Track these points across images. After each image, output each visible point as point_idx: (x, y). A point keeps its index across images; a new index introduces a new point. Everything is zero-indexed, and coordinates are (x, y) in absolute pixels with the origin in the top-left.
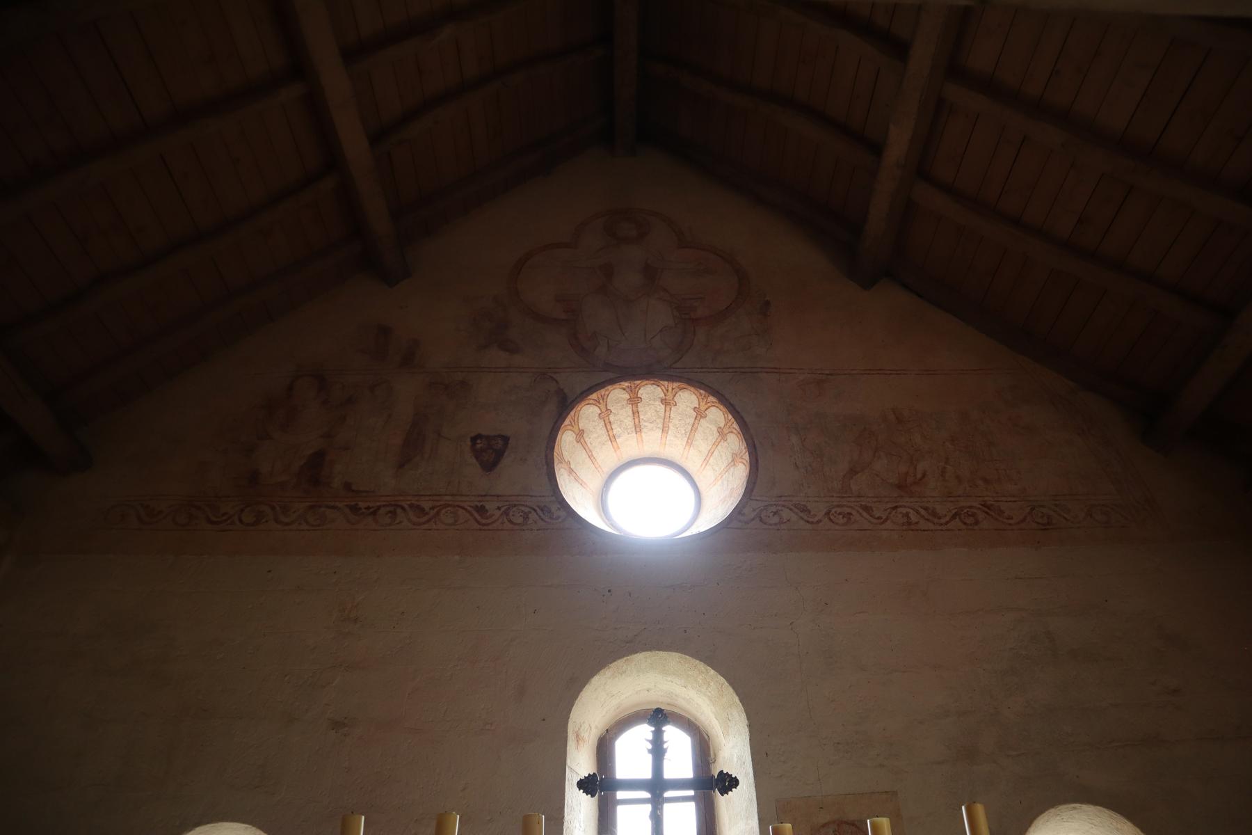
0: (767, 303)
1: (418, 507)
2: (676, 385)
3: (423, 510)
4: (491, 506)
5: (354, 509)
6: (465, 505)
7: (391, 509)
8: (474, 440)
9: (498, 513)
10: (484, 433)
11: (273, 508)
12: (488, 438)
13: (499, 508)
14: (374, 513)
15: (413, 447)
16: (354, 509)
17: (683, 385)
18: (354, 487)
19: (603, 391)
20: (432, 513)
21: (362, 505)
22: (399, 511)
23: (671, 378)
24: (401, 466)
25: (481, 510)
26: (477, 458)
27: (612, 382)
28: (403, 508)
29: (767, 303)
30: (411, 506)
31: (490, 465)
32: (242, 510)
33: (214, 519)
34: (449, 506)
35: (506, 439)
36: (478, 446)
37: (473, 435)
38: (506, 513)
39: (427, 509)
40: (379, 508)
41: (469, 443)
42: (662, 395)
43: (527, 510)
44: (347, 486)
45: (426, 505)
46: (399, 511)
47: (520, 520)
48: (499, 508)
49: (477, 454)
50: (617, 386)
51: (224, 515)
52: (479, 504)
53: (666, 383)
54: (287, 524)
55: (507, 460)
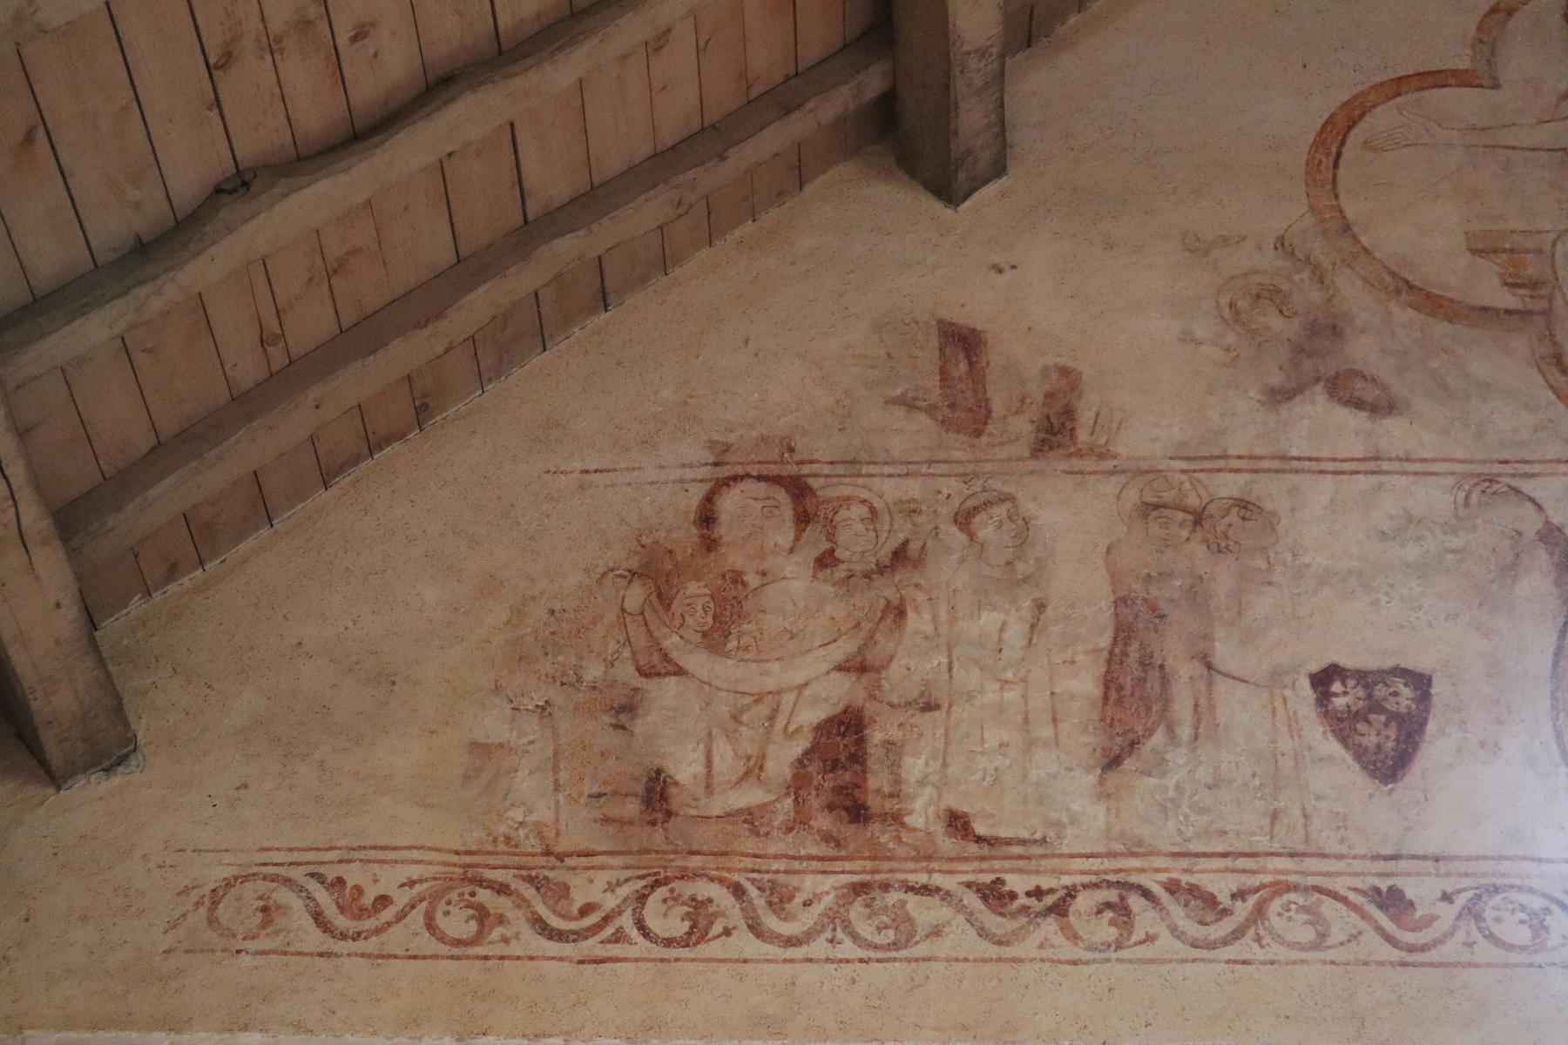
1: (1193, 890)
3: (1211, 901)
4: (1421, 889)
5: (995, 895)
6: (1339, 885)
7: (1112, 895)
8: (1323, 680)
9: (1448, 912)
10: (1347, 662)
11: (738, 891)
12: (1363, 677)
13: (1447, 897)
14: (1059, 909)
15: (1132, 707)
16: (995, 895)
18: (980, 829)
20: (1243, 909)
21: (1014, 882)
22: (1135, 902)
24: (1112, 762)
25: (1392, 900)
26: (1344, 741)
28: (1146, 894)
30: (1172, 888)
31: (1390, 766)
32: (642, 898)
33: (555, 922)
34: (1295, 888)
35: (1421, 683)
36: (1339, 702)
37: (1315, 667)
38: (1472, 912)
39: (1224, 899)
40: (1071, 892)
41: (1307, 692)
43: (1536, 903)
44: (958, 823)
45: (1221, 886)
46: (1135, 902)
47: (1523, 935)
48: (1447, 897)
49: (1343, 726)
51: (586, 910)
52: (1384, 885)
54: (791, 942)
55: (1436, 747)
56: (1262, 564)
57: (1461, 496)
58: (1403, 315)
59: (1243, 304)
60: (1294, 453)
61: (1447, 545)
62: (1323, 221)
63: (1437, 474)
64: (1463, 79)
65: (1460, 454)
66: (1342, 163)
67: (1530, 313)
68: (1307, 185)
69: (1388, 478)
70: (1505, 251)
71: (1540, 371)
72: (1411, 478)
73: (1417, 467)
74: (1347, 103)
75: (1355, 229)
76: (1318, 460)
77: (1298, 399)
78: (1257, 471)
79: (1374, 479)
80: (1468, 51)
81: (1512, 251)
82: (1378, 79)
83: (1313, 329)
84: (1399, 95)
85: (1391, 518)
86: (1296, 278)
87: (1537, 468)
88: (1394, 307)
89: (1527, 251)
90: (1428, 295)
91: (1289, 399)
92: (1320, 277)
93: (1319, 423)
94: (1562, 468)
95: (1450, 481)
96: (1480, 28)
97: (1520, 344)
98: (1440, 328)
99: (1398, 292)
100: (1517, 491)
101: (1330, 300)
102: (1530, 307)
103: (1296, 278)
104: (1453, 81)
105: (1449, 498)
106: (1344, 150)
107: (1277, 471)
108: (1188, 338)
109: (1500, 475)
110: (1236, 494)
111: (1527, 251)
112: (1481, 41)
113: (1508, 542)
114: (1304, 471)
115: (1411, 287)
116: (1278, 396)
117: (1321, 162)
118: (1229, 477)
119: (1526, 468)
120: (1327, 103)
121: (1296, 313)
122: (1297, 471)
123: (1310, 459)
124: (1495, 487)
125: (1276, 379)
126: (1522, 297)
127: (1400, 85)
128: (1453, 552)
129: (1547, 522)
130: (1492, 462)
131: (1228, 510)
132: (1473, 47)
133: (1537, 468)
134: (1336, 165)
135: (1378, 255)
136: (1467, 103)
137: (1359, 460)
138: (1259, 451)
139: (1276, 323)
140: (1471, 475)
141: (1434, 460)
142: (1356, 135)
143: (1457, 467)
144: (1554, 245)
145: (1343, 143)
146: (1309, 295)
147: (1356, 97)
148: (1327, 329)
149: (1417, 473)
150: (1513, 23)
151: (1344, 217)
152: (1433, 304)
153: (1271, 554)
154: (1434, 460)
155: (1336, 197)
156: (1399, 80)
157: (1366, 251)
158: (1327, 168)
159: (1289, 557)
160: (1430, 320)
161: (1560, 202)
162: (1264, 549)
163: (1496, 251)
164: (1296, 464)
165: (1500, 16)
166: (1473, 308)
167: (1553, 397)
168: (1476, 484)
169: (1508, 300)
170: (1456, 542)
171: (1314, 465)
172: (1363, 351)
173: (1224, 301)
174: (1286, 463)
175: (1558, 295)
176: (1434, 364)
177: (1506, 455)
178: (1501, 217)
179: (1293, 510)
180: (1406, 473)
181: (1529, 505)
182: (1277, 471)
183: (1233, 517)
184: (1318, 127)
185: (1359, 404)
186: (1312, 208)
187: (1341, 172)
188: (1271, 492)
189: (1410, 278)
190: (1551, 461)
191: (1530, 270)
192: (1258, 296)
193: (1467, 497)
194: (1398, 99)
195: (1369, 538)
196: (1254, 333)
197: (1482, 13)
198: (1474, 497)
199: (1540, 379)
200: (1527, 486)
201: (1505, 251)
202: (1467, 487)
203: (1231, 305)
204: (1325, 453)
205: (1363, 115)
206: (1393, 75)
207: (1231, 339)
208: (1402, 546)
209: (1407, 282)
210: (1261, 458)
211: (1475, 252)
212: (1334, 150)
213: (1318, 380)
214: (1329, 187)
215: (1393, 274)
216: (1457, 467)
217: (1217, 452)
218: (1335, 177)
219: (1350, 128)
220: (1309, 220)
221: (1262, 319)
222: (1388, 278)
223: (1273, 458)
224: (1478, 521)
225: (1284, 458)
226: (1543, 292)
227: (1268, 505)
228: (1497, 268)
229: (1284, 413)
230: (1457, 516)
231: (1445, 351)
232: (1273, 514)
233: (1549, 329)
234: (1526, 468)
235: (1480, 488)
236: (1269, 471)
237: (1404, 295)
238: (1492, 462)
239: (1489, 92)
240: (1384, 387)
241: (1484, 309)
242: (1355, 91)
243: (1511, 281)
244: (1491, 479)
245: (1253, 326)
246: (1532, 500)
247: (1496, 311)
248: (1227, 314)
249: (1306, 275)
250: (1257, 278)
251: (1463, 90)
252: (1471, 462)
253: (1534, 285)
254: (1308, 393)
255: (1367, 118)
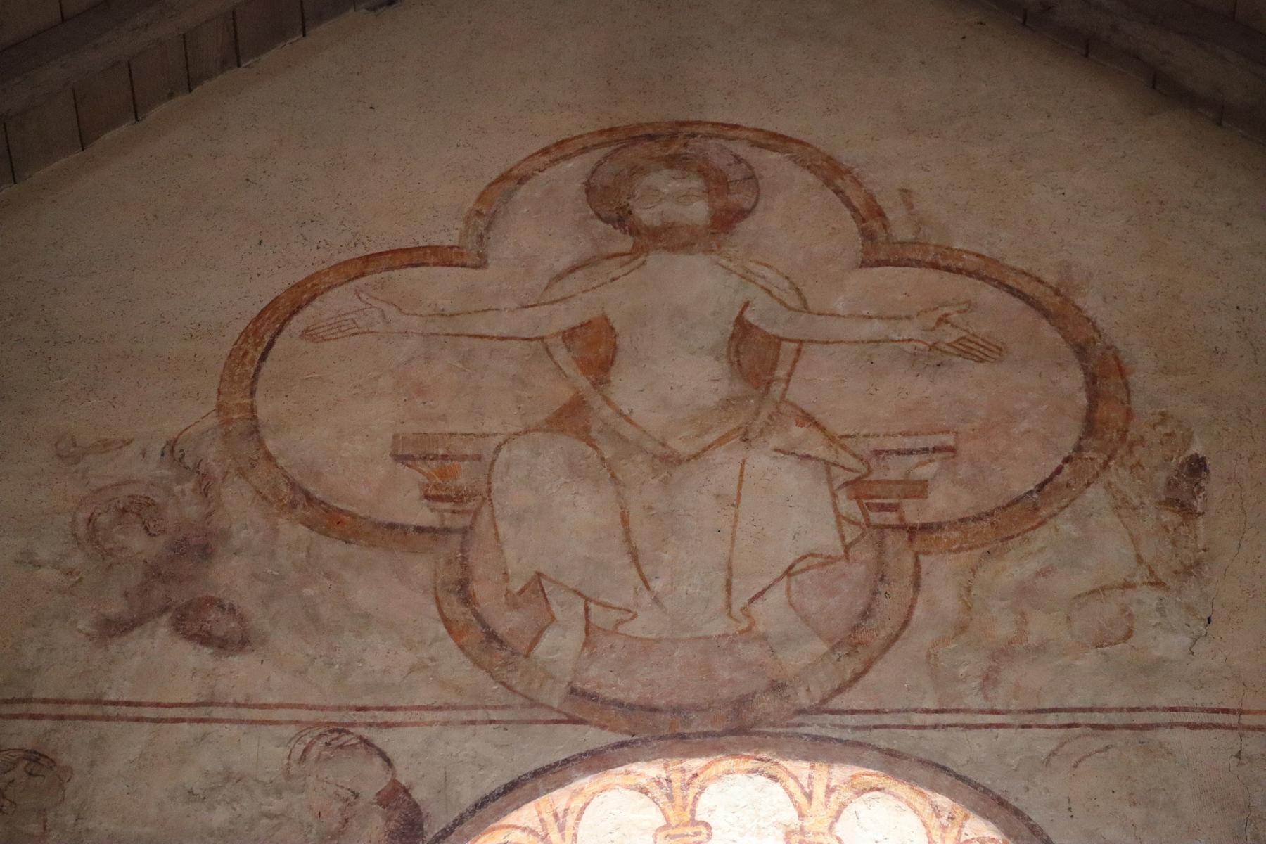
0: (1197, 466)
2: (841, 773)
17: (871, 776)
19: (559, 798)
23: (821, 749)
27: (596, 761)
29: (1197, 466)
42: (790, 816)
50: (615, 776)
53: (801, 768)
56: (35, 828)
57: (300, 748)
58: (293, 532)
59: (103, 520)
60: (112, 696)
61: (265, 808)
62: (229, 422)
63: (277, 723)
64: (443, 256)
65: (311, 700)
66: (272, 354)
67: (447, 530)
68: (222, 380)
69: (216, 726)
70: (436, 457)
71: (437, 600)
72: (244, 727)
73: (257, 714)
74: (297, 285)
75: (263, 432)
76: (139, 704)
77: (136, 632)
78: (62, 718)
79: (199, 728)
80: (461, 225)
81: (444, 457)
82: (344, 257)
83: (180, 549)
84: (363, 275)
85: (207, 774)
86: (177, 489)
87: (399, 717)
88: (283, 524)
89: (464, 458)
90: (328, 510)
91: (125, 631)
92: (205, 486)
93: (164, 662)
94: (7, 710)
95: (291, 731)
96: (480, 199)
97: (422, 568)
98: (332, 549)
99: (293, 505)
100: (367, 743)
101: (210, 514)
102: (447, 523)
103: (177, 489)
104: (432, 260)
105: (282, 752)
106: (278, 339)
107: (85, 718)
108: (29, 560)
109: (353, 724)
110: (29, 745)
111: (464, 458)
112: (479, 213)
113: (340, 805)
114: (118, 718)
115: (309, 498)
116: (113, 628)
117: (246, 353)
118: (27, 724)
119: (388, 716)
120: (278, 283)
121: (163, 531)
122: (108, 718)
123: (129, 704)
124: (345, 738)
125: (116, 607)
126: (441, 512)
127: (368, 262)
128: (270, 816)
129: (394, 781)
130: (349, 708)
131: (16, 763)
132: (467, 220)
133: (399, 717)
134: (263, 357)
135: (281, 462)
136: (441, 285)
137: (189, 705)
138: (72, 694)
139: (138, 543)
140: (318, 724)
141: (278, 706)
142: (297, 324)
143: (304, 715)
144: (498, 449)
145: (279, 331)
146: (186, 507)
147: (311, 278)
148: (199, 547)
149: (253, 722)
150: (524, 190)
151: (255, 417)
152: (333, 520)
153: (50, 816)
154: (278, 706)
155: (252, 394)
156: (367, 259)
157: (269, 457)
158: (252, 361)
159: (70, 820)
160: (323, 539)
161: (519, 399)
162: (44, 811)
163: (425, 458)
164: (110, 710)
165: (508, 185)
166: (377, 525)
167: (443, 630)
168: (320, 736)
169: (425, 516)
170: (276, 805)
171: (131, 711)
172: (230, 576)
173: (83, 516)
174: (99, 708)
175: (486, 510)
176: (308, 591)
177: (368, 701)
178: (443, 417)
179: (92, 764)
180: (241, 722)
181: (378, 761)
182: (85, 718)
183: (19, 773)
184: (257, 311)
185: (205, 639)
186: (219, 407)
187: (268, 366)
188: (71, 745)
189: (311, 489)
190: (419, 708)
191: (462, 481)
192: (124, 511)
193: (305, 751)
194: (362, 281)
195: (172, 798)
196: (109, 553)
197: (488, 181)
198: (314, 751)
199: (434, 609)
200: (379, 738)
201: (436, 457)
202: (308, 739)
203: (91, 521)
204: (150, 698)
205: (313, 298)
206: (361, 252)
207: (77, 560)
208: (211, 808)
209: (307, 495)
210: (71, 702)
211: (399, 458)
212: (267, 339)
213: (165, 610)
214: (247, 382)
215: (293, 485)
216: (304, 715)
217: (22, 695)
218: (258, 369)
219: (293, 313)
220: (212, 421)
221: (122, 537)
222: (285, 489)
223: (85, 702)
224: (311, 780)
225: (97, 702)
226: (469, 506)
227: (64, 759)
228: (421, 477)
229: (113, 649)
230: (289, 776)
231: (328, 576)
232: (68, 769)
233: (462, 551)
234: (388, 716)
235: (325, 740)
236: (76, 717)
237: (299, 510)
238: (349, 708)
239: (471, 272)
240: (242, 618)
241: (392, 526)
242: (312, 271)
243: (434, 492)
244: (341, 730)
245: (107, 546)
246: (382, 754)
247: (404, 528)
248: (82, 530)
249: (189, 486)
250: (129, 490)
251: (439, 270)
252: (323, 708)
253: (460, 498)
254: (149, 625)
255: (317, 303)
